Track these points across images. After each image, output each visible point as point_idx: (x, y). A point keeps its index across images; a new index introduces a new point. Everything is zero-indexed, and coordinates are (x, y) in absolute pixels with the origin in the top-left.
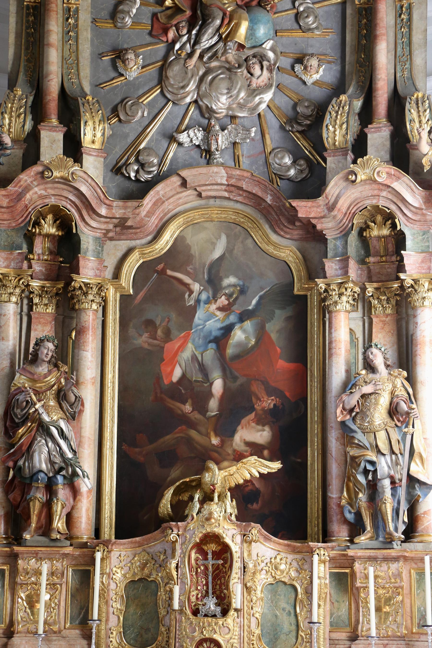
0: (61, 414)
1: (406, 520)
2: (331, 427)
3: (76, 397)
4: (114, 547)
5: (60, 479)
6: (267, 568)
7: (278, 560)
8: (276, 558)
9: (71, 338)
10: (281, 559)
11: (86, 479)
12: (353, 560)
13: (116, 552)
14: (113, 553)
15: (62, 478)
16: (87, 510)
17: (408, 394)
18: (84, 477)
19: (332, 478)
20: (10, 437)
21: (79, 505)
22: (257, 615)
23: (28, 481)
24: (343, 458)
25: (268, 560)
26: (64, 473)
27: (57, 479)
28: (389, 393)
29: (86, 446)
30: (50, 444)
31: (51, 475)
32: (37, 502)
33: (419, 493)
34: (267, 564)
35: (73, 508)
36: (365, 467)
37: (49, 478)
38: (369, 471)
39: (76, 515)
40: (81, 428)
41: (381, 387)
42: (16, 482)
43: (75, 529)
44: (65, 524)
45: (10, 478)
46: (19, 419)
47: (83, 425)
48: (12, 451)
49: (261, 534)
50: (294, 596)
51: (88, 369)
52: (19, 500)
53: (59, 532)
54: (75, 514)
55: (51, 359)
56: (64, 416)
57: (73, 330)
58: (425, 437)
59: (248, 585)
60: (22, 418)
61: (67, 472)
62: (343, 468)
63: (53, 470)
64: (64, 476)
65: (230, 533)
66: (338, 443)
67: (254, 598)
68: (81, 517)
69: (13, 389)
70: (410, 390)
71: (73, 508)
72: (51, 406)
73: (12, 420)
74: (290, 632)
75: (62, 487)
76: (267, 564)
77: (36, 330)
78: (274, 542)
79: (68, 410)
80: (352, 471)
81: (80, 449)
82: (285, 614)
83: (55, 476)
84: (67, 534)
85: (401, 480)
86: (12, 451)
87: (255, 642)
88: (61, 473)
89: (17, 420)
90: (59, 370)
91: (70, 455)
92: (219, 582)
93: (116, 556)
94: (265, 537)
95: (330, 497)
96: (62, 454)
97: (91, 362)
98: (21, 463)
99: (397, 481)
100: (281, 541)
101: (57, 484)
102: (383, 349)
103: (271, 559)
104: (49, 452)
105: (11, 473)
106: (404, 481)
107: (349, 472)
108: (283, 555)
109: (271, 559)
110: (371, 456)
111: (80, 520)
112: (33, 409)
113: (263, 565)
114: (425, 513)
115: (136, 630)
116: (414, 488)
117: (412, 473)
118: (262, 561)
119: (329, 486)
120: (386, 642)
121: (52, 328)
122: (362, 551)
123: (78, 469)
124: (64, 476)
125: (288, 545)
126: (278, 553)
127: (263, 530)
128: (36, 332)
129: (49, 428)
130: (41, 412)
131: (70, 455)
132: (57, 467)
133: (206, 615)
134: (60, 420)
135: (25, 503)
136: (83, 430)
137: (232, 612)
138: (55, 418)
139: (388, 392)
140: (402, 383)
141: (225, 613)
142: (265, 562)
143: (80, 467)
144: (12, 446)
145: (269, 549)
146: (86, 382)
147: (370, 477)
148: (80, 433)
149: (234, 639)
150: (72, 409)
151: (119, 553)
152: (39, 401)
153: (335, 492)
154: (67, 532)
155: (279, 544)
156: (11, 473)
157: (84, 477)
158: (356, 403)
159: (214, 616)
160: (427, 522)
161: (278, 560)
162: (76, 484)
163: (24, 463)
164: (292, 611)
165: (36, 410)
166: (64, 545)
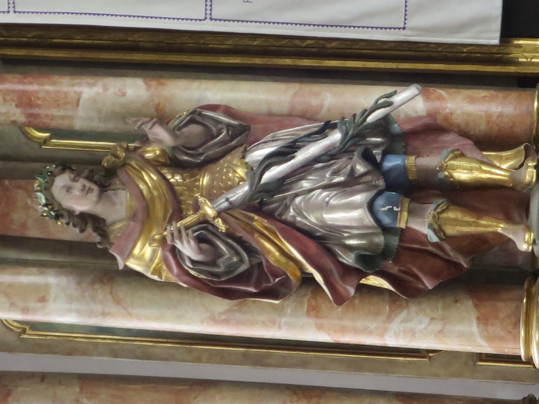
0: (234, 158)
3: (192, 121)
9: (45, 141)
11: (397, 99)
16: (472, 100)
18: (390, 104)
20: (285, 283)
21: (458, 118)
23: (395, 241)
26: (377, 153)
27: (391, 169)
29: (314, 102)
30: (306, 184)
32: (444, 215)
35: (465, 134)
42: (394, 269)
44: (504, 154)
45: (384, 284)
46: (241, 261)
47: (264, 109)
48: (318, 278)
51: (124, 95)
52: (439, 263)
53: (521, 166)
55: (95, 183)
56: (239, 152)
57: (26, 134)
60: (237, 254)
61: (377, 145)
63: (369, 178)
64: (385, 154)
68: (489, 116)
69: (166, 276)
71: (465, 134)
72: (212, 180)
73: (244, 278)
77: (24, 226)
79: (223, 142)
81: (320, 116)
83: (385, 174)
84: (526, 148)
86: (318, 278)
88: (378, 158)
89: (243, 268)
90: (124, 164)
91: (336, 137)
97: (106, 89)
98: (349, 259)
104: (325, 187)
105: (374, 281)
111: (494, 118)
112: (219, 223)
121: (19, 187)
123: (371, 119)
124: (385, 154)
128: (30, 224)
129: (266, 184)
130: (226, 204)
131: (336, 137)
132: (360, 168)
134: (247, 160)
135: (447, 247)
136: (276, 109)
138: (241, 172)
143: (367, 113)
144: (309, 280)
146: (156, 100)
148: (282, 115)
150: (219, 133)
152: (197, 208)
154: (522, 147)
156: (374, 281)
157: (390, 104)
162: (407, 127)
163: (350, 248)
165: (219, 214)
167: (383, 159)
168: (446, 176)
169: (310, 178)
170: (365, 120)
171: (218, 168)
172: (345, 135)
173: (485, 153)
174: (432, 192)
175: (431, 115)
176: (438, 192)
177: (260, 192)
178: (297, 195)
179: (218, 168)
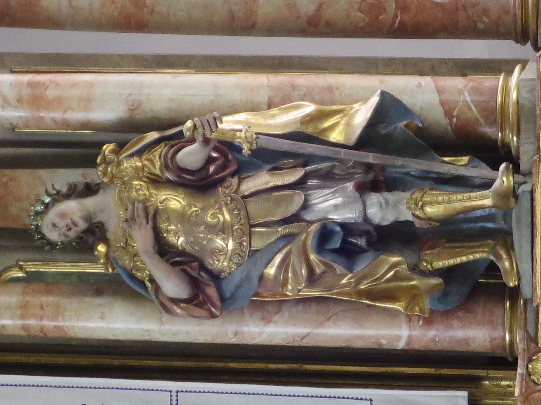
1: (465, 159)
2: (236, 334)
17: (157, 142)
19: (360, 337)
24: (314, 307)
28: (156, 188)
33: (402, 124)
36: (334, 251)
38: (344, 241)
41: (141, 206)
58: (266, 106)
62: (338, 308)
66: (276, 318)
70: (153, 136)
80: (345, 285)
85: (369, 167)
95: (408, 344)
99: (371, 176)
102: (47, 200)
106: (371, 158)
107: (348, 294)
110: (308, 234)
114: (449, 114)
116: (388, 137)
117: (353, 139)
119: (380, 344)
139: (153, 191)
140: (132, 155)
147: (361, 242)
153: (395, 332)
158: (178, 268)
160: (471, 109)
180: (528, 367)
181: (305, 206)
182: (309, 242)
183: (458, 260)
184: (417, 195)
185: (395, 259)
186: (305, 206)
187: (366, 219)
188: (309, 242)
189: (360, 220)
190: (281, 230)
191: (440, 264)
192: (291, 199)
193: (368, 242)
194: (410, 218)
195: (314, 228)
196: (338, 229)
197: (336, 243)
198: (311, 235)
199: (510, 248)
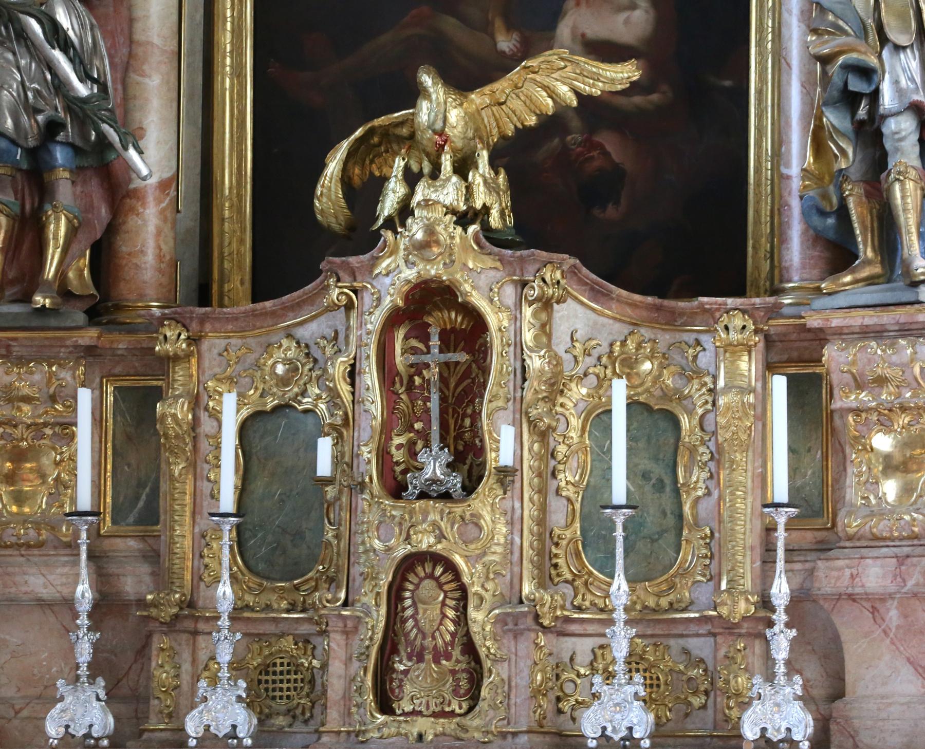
4: (208, 327)
5: (60, 155)
6: (598, 370)
7: (631, 345)
8: (624, 343)
10: (639, 346)
12: (820, 337)
13: (217, 341)
14: (205, 345)
15: (69, 151)
22: (569, 492)
25: (605, 348)
31: (31, 143)
34: (599, 359)
37: (31, 153)
39: (124, 249)
40: (131, 21)
43: (122, 284)
49: (581, 282)
50: (672, 441)
54: (124, 247)
59: (533, 413)
65: (483, 281)
67: (562, 449)
74: (661, 534)
75: (67, 175)
76: (599, 359)
78: (619, 300)
82: (648, 488)
87: (561, 561)
92: (469, 411)
93: (216, 351)
94: (592, 289)
96: (60, 86)
100: (637, 297)
101: (52, 168)
103: (611, 345)
108: (646, 333)
109: (611, 345)
110: (865, 53)
113: (589, 360)
115: (270, 538)
118: (587, 353)
120: (906, 550)
122: (841, 313)
125: (658, 308)
126: (631, 328)
127: (585, 270)
133: (423, 495)
137: (488, 483)
141: (469, 489)
142: (595, 353)
145: (606, 320)
147: (862, 112)
149: (494, 553)
151: (223, 343)
154: (93, 291)
155: (634, 305)
159: (446, 496)
161: (631, 345)
164: (668, 481)
166: (69, 323)
167: (62, 143)
168: (47, 212)
169: (33, 65)
170: (104, 122)
171: (727, 83)
172: (85, 101)
173: (88, 252)
174: (37, 200)
175: (136, 194)
176: (36, 204)
177: (9, 14)
178: (14, 54)
179: (727, 83)
180: (735, 309)
181: (898, 48)
182: (855, 55)
183: (856, 225)
184: (913, 174)
185: (850, 152)
186: (898, 48)
187: (884, 117)
188: (855, 55)
189: (881, 110)
190: (870, 22)
191: (851, 204)
192: (906, 30)
193: (862, 123)
194: (890, 167)
195: (873, 61)
196: (873, 87)
197: (856, 85)
198: (863, 57)
199: (871, 281)
